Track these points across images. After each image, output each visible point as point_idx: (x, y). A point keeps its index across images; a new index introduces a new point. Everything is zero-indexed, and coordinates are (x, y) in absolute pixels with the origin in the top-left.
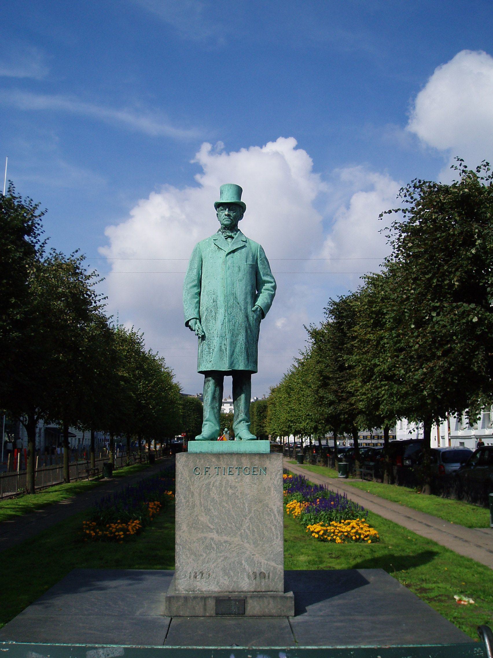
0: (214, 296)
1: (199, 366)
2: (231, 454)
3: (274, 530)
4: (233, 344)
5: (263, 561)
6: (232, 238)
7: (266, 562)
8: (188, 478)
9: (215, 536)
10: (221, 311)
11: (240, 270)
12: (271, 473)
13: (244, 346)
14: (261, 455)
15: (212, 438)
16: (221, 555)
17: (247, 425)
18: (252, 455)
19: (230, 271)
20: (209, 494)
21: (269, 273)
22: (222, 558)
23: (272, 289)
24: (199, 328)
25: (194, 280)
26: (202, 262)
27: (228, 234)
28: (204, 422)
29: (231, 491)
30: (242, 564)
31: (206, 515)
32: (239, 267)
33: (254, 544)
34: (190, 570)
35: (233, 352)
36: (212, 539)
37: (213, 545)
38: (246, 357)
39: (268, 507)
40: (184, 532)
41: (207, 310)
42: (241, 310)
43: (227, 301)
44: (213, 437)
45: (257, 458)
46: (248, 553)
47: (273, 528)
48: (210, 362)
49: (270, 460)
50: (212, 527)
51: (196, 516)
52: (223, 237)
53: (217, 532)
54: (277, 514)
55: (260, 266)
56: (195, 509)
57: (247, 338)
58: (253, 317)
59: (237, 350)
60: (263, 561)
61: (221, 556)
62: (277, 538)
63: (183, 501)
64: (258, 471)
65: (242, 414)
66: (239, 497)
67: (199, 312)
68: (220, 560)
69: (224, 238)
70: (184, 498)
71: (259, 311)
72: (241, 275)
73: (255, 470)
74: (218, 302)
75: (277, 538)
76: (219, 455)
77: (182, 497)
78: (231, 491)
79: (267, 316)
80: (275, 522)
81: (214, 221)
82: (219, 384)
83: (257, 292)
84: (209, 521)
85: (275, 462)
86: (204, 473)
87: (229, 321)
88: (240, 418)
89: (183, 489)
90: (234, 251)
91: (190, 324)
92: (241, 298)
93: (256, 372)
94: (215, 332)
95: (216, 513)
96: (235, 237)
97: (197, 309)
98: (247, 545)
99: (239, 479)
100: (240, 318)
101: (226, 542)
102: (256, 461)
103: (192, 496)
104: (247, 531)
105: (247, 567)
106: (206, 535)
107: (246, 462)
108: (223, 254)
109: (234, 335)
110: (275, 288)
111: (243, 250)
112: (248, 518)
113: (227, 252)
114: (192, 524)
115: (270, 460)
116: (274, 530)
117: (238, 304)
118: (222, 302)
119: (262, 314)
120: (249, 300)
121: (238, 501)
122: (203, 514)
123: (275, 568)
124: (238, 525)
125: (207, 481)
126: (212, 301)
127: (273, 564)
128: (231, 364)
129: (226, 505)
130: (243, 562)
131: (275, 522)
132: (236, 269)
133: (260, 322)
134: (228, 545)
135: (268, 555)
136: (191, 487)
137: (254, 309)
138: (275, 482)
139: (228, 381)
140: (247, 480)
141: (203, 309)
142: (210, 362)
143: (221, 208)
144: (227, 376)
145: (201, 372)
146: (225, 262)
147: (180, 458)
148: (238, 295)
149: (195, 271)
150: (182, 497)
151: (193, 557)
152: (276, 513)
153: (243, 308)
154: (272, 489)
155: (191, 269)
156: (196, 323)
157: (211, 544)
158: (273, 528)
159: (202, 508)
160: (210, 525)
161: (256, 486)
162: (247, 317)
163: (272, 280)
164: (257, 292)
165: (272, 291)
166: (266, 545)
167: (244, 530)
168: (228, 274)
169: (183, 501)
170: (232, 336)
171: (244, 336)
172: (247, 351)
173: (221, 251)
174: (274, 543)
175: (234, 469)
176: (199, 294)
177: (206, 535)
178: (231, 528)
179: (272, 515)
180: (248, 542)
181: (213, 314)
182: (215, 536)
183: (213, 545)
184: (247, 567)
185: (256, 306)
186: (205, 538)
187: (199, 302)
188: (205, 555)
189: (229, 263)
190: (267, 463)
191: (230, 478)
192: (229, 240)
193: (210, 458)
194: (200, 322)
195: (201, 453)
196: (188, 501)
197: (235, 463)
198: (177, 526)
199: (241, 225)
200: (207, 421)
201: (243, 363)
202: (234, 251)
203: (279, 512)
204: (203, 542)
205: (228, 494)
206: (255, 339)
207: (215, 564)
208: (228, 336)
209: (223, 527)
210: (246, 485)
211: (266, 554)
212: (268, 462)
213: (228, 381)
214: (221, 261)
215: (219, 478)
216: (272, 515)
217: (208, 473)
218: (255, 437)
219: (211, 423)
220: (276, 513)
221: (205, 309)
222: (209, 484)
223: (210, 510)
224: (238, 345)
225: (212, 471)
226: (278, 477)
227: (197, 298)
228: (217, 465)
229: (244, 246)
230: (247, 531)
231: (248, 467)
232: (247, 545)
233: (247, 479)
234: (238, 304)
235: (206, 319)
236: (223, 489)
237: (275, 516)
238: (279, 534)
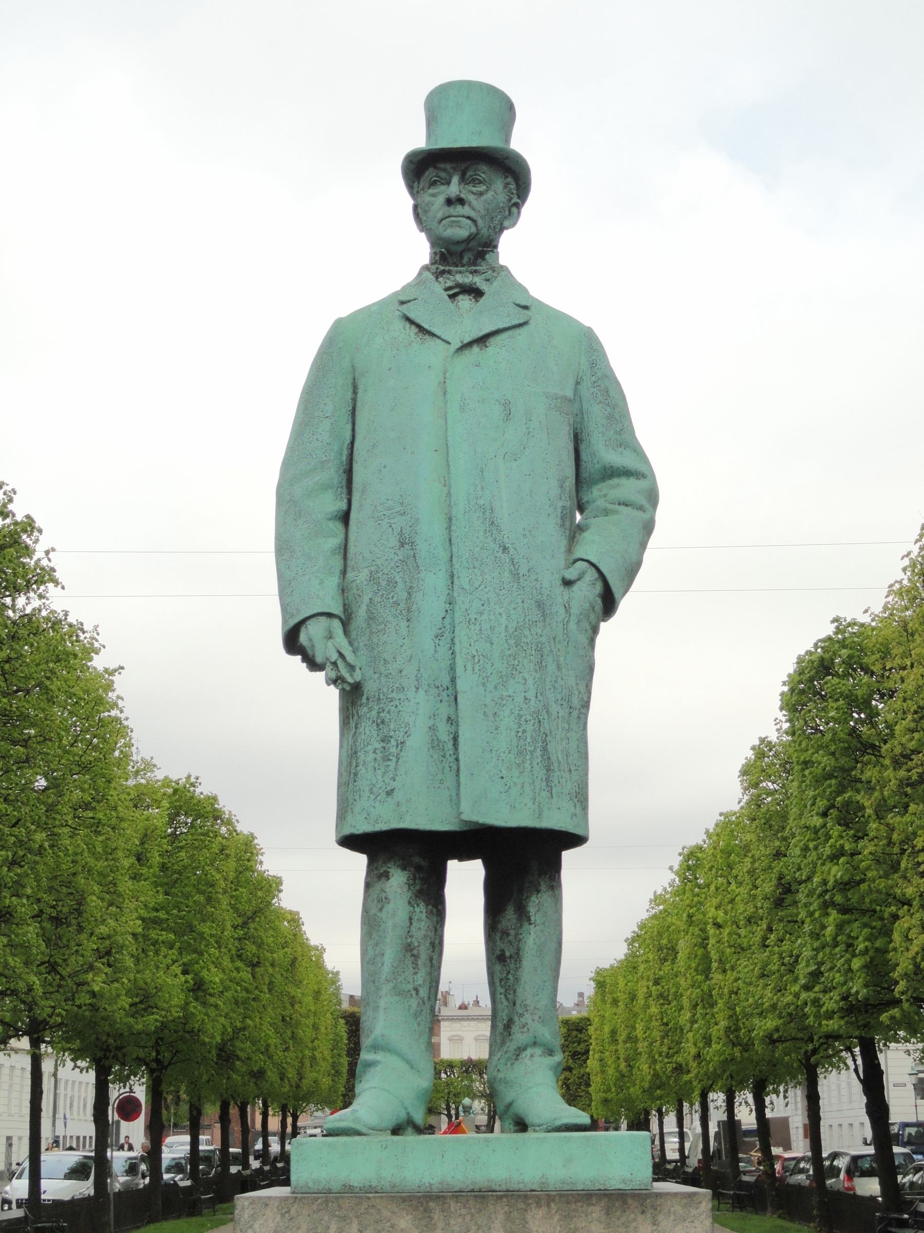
1: (342, 815)
2: (481, 1196)
6: (476, 293)
11: (508, 416)
13: (529, 728)
14: (616, 1200)
18: (573, 1199)
24: (341, 655)
26: (355, 392)
27: (459, 278)
38: (540, 772)
41: (372, 578)
44: (403, 1116)
45: (596, 1211)
48: (389, 793)
49: (655, 1223)
52: (438, 288)
58: (567, 609)
69: (445, 295)
74: (422, 546)
76: (425, 1201)
79: (625, 605)
82: (431, 892)
83: (578, 517)
90: (482, 340)
91: (303, 638)
93: (576, 840)
97: (333, 582)
110: (653, 497)
113: (457, 344)
115: (655, 1223)
117: (505, 549)
120: (551, 533)
126: (394, 542)
133: (595, 630)
139: (466, 881)
141: (359, 577)
142: (389, 793)
143: (430, 173)
144: (461, 859)
145: (350, 842)
147: (253, 1217)
156: (330, 636)
164: (578, 517)
165: (641, 508)
171: (530, 681)
172: (545, 749)
173: (431, 342)
176: (345, 518)
181: (401, 593)
192: (465, 301)
193: (385, 1213)
194: (346, 632)
195: (348, 1190)
199: (511, 249)
200: (375, 1048)
206: (576, 702)
213: (466, 881)
221: (364, 575)
234: (505, 549)
235: (371, 618)
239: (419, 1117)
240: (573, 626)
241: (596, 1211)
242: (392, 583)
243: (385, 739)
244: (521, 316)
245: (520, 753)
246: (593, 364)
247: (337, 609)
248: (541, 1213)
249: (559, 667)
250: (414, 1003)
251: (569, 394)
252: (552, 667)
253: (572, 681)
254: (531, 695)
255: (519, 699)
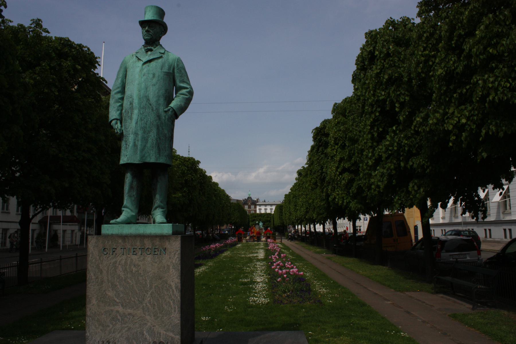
0: (130, 99)
3: (172, 304)
4: (145, 140)
5: (162, 332)
7: (165, 332)
8: (98, 258)
9: (120, 309)
10: (136, 112)
12: (170, 252)
14: (162, 237)
15: (128, 222)
16: (126, 326)
17: (162, 211)
18: (153, 237)
19: (145, 77)
20: (116, 271)
21: (185, 80)
22: (126, 329)
23: (187, 94)
25: (119, 88)
27: (148, 47)
28: (123, 209)
29: (134, 269)
30: (143, 334)
31: (112, 290)
32: (154, 75)
33: (154, 316)
34: (98, 339)
35: (145, 146)
36: (118, 312)
37: (119, 317)
39: (167, 283)
40: (93, 305)
41: (125, 111)
42: (153, 110)
43: (140, 103)
45: (158, 239)
46: (149, 324)
47: (171, 302)
49: (169, 242)
50: (118, 301)
51: (104, 291)
53: (122, 305)
54: (175, 291)
55: (177, 75)
56: (103, 285)
57: (158, 134)
59: (149, 145)
60: (162, 332)
61: (125, 327)
62: (175, 311)
63: (93, 277)
64: (158, 251)
65: (158, 201)
66: (142, 274)
67: (121, 114)
68: (124, 331)
70: (94, 275)
71: (172, 112)
72: (154, 81)
73: (156, 250)
74: (134, 104)
75: (175, 311)
77: (92, 274)
78: (134, 269)
80: (173, 297)
81: (138, 38)
84: (115, 295)
85: (174, 243)
86: (111, 253)
87: (141, 120)
88: (156, 205)
89: (93, 267)
90: (150, 61)
92: (153, 100)
94: (131, 130)
95: (122, 289)
96: (154, 49)
97: (119, 112)
98: (148, 317)
99: (142, 258)
100: (152, 117)
101: (129, 314)
102: (157, 242)
103: (101, 273)
104: (148, 304)
105: (148, 337)
106: (112, 308)
107: (148, 244)
108: (140, 64)
109: (146, 131)
110: (191, 93)
111: (160, 60)
112: (149, 293)
114: (101, 298)
116: (172, 304)
118: (137, 103)
119: (176, 115)
120: (162, 101)
121: (140, 278)
122: (110, 289)
123: (172, 338)
124: (140, 299)
125: (114, 260)
126: (129, 104)
127: (171, 334)
128: (142, 157)
129: (130, 281)
130: (145, 332)
131: (173, 297)
132: (151, 76)
134: (131, 317)
135: (167, 327)
136: (100, 265)
137: (166, 109)
138: (174, 261)
140: (149, 259)
146: (142, 70)
147: (91, 240)
148: (151, 97)
149: (120, 81)
150: (92, 274)
151: (101, 327)
152: (174, 288)
153: (154, 109)
154: (171, 267)
155: (117, 79)
156: (117, 123)
157: (117, 316)
158: (171, 302)
159: (110, 284)
160: (116, 299)
161: (156, 265)
162: (159, 117)
163: (188, 86)
165: (187, 95)
166: (165, 318)
167: (146, 304)
168: (143, 79)
169: (93, 277)
170: (144, 132)
172: (158, 146)
174: (173, 315)
175: (138, 249)
176: (122, 99)
177: (112, 308)
178: (134, 302)
179: (171, 290)
180: (149, 315)
181: (130, 114)
182: (120, 309)
183: (119, 317)
184: (148, 337)
185: (169, 108)
186: (112, 311)
187: (122, 106)
188: (111, 326)
189: (145, 71)
190: (167, 245)
191: (134, 257)
192: (149, 53)
194: (121, 123)
195: (112, 235)
196: (97, 278)
197: (138, 243)
198: (87, 300)
201: (154, 157)
202: (150, 61)
203: (176, 288)
204: (110, 314)
205: (132, 272)
207: (120, 334)
208: (140, 133)
209: (128, 301)
210: (148, 263)
211: (165, 326)
212: (167, 243)
214: (138, 69)
215: (124, 257)
216: (171, 290)
217: (114, 253)
218: (165, 220)
219: (127, 210)
220: (174, 288)
222: (115, 262)
223: (116, 286)
224: (150, 141)
225: (119, 251)
226: (176, 256)
227: (120, 102)
228: (123, 246)
229: (161, 57)
230: (148, 304)
231: (150, 247)
232: (148, 317)
233: (149, 258)
234: (151, 105)
236: (127, 267)
237: (173, 291)
238: (177, 308)
239: (133, 221)
240: (166, 120)
241: (158, 239)
242: (128, 112)
243: (126, 145)
244: (161, 55)
245: (153, 147)
246: (178, 65)
247: (118, 118)
248: (147, 239)
249: (163, 129)
250: (133, 198)
251: (171, 71)
252: (161, 129)
253: (166, 132)
254: (155, 135)
255: (153, 136)
